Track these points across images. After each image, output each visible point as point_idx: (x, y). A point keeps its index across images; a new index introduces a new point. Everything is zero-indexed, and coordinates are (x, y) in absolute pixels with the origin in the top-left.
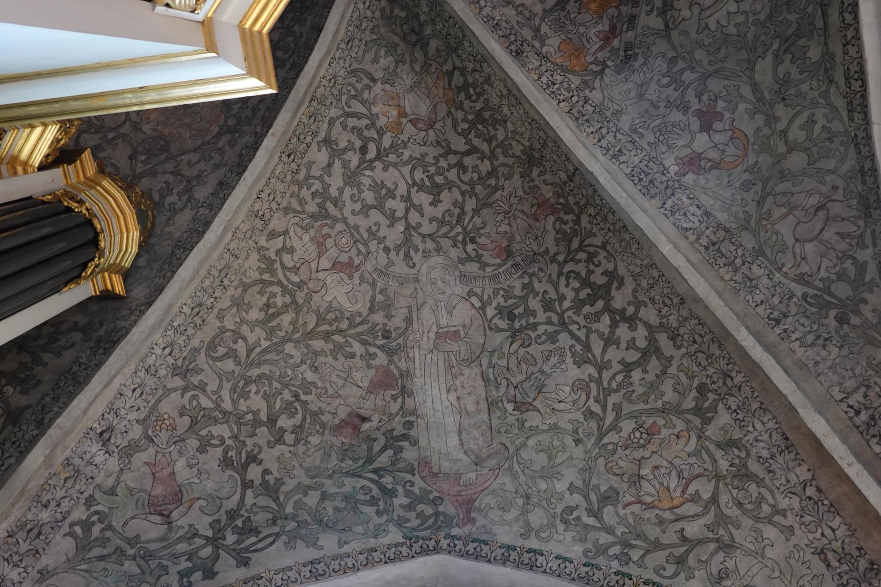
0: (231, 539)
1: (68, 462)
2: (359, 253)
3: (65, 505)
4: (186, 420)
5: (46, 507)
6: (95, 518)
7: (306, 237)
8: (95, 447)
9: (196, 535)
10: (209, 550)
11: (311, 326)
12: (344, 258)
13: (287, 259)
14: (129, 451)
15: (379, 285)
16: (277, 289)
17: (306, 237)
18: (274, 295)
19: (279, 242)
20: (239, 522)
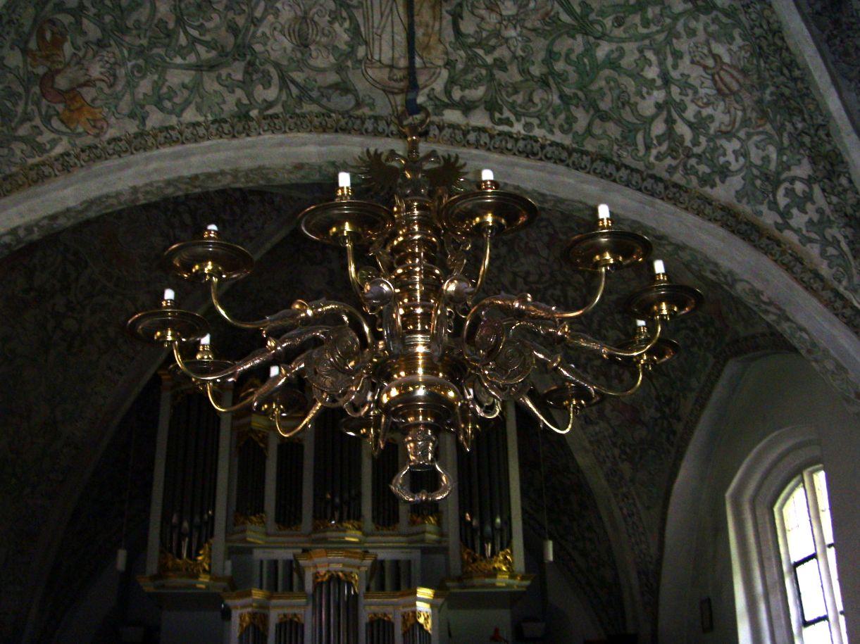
0: (667, 410)
1: (591, 442)
2: (546, 227)
3: (609, 454)
4: (602, 378)
5: (605, 461)
6: (623, 447)
7: (523, 260)
8: (590, 429)
9: (656, 420)
10: (665, 422)
11: (582, 280)
12: (546, 239)
13: (531, 279)
14: (601, 414)
15: (573, 225)
16: (549, 292)
17: (523, 260)
18: (553, 294)
19: (520, 280)
20: (663, 400)
